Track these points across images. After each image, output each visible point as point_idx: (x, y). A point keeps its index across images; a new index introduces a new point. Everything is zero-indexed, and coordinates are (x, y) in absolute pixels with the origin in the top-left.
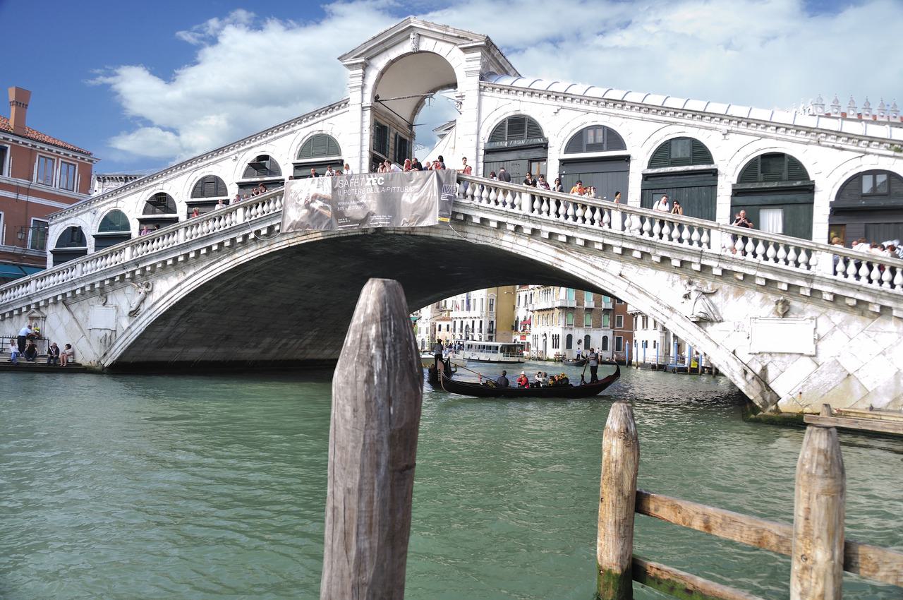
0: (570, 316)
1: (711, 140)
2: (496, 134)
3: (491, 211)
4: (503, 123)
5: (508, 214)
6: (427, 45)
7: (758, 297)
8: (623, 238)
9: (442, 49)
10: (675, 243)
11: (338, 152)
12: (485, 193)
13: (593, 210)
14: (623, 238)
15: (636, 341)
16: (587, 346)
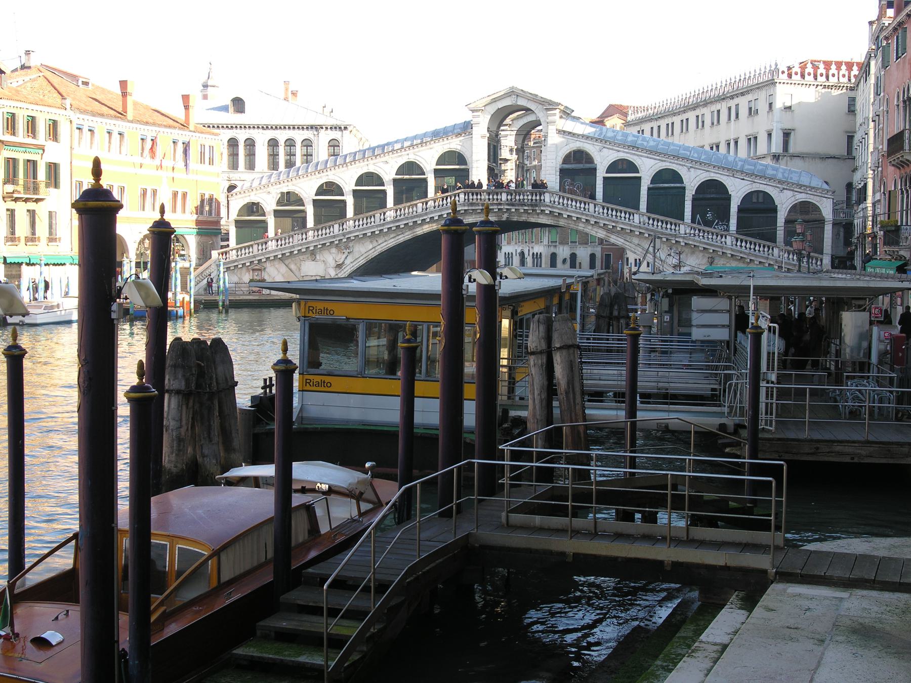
0: (554, 231)
1: (682, 171)
2: (567, 159)
3: (573, 212)
4: (570, 153)
5: (582, 214)
6: (522, 102)
7: (701, 254)
8: (640, 228)
9: (532, 106)
10: (664, 231)
11: (466, 164)
12: (570, 202)
13: (625, 213)
14: (640, 228)
15: (627, 259)
16: (573, 265)
